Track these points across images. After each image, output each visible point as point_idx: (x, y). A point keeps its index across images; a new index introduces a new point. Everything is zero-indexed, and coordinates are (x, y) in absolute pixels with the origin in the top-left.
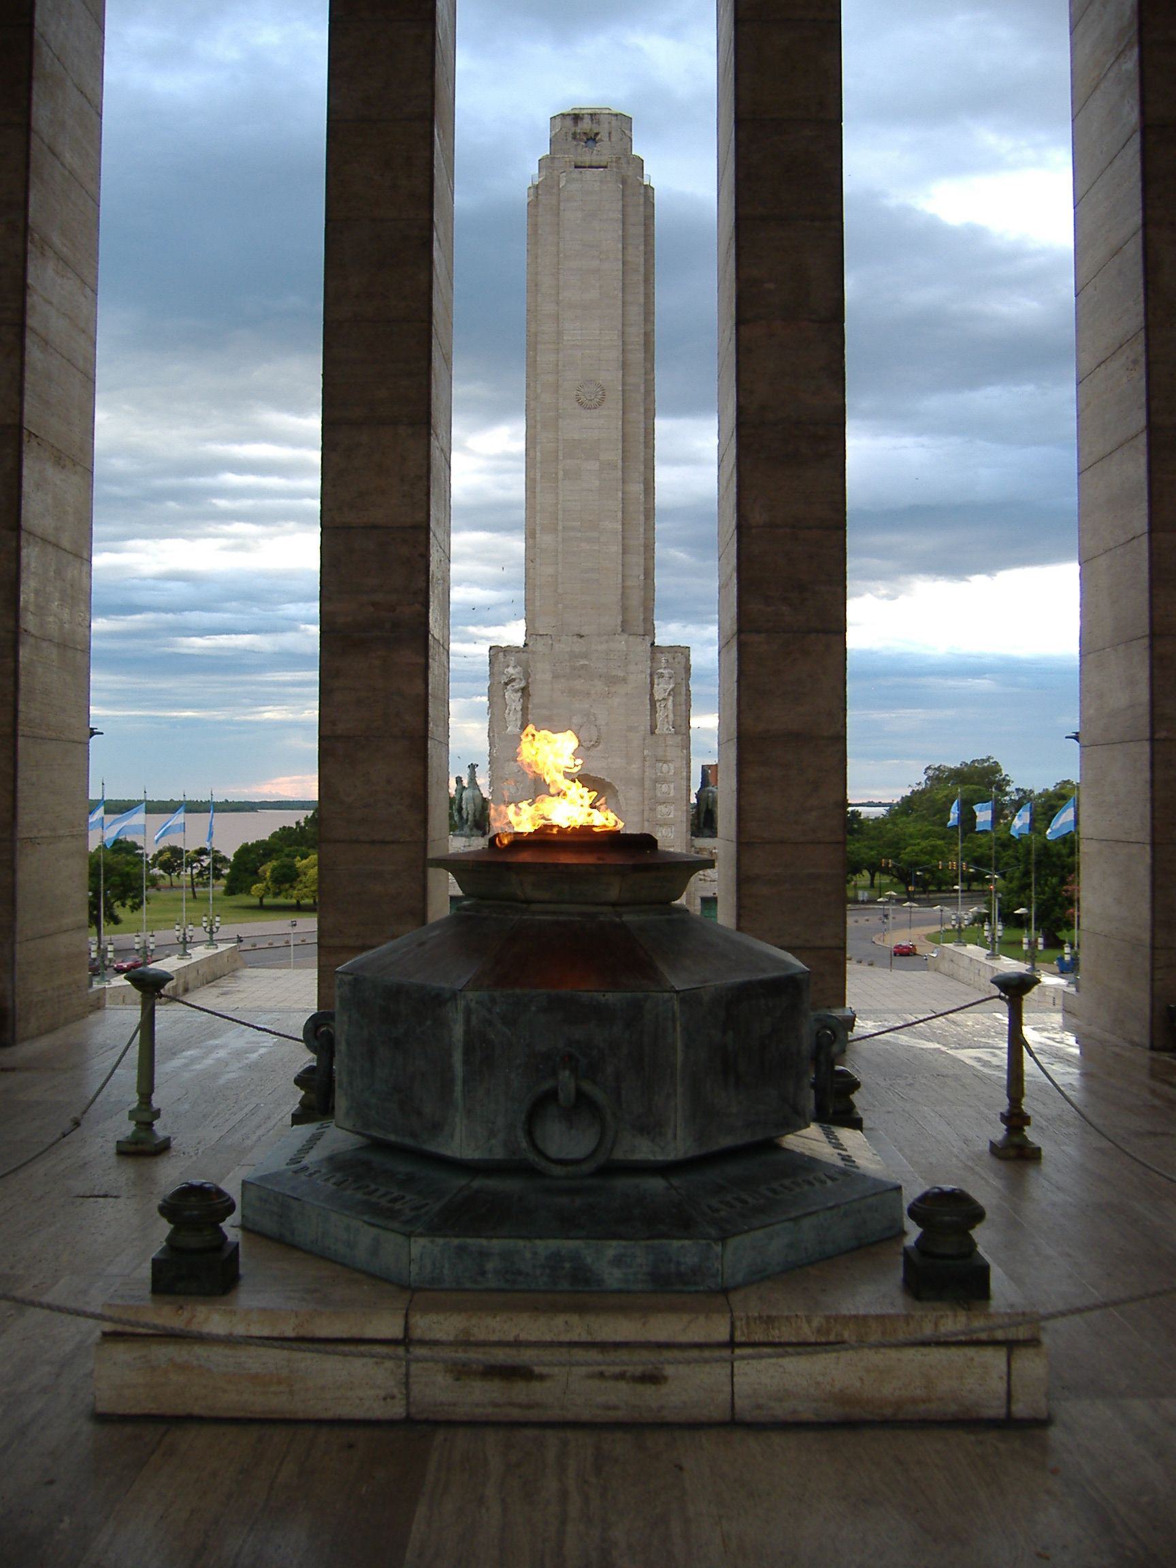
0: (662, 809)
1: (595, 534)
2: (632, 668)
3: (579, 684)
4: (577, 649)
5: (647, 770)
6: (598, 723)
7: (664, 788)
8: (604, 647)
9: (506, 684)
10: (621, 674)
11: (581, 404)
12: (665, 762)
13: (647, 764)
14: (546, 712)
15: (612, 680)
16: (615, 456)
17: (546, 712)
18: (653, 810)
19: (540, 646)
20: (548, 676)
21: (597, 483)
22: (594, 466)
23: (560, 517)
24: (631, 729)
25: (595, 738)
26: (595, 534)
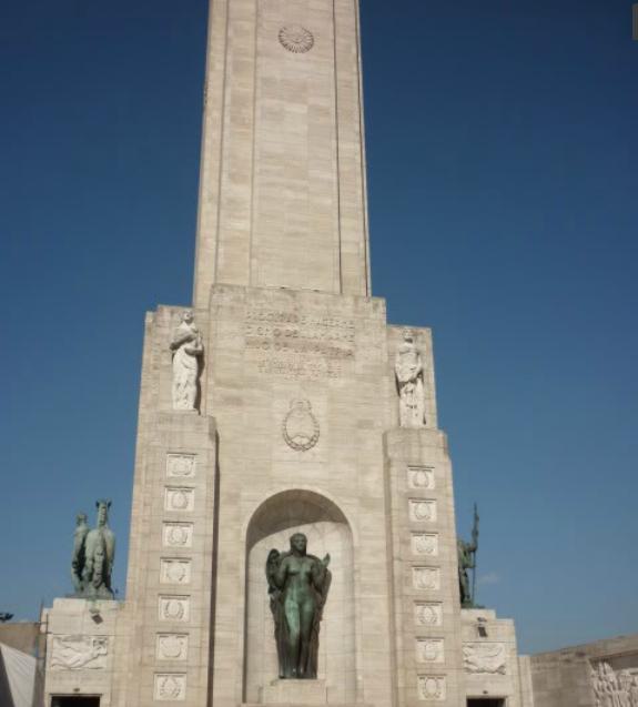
0: (417, 541)
1: (304, 183)
2: (362, 339)
3: (283, 356)
4: (281, 308)
5: (393, 478)
6: (313, 411)
7: (422, 508)
8: (322, 307)
9: (175, 347)
10: (346, 346)
11: (285, 45)
12: (421, 468)
13: (394, 471)
14: (234, 392)
15: (336, 354)
16: (328, 103)
17: (234, 392)
18: (406, 543)
19: (227, 299)
20: (238, 343)
21: (306, 128)
22: (299, 109)
23: (257, 157)
24: (362, 424)
25: (312, 434)
26: (304, 183)
